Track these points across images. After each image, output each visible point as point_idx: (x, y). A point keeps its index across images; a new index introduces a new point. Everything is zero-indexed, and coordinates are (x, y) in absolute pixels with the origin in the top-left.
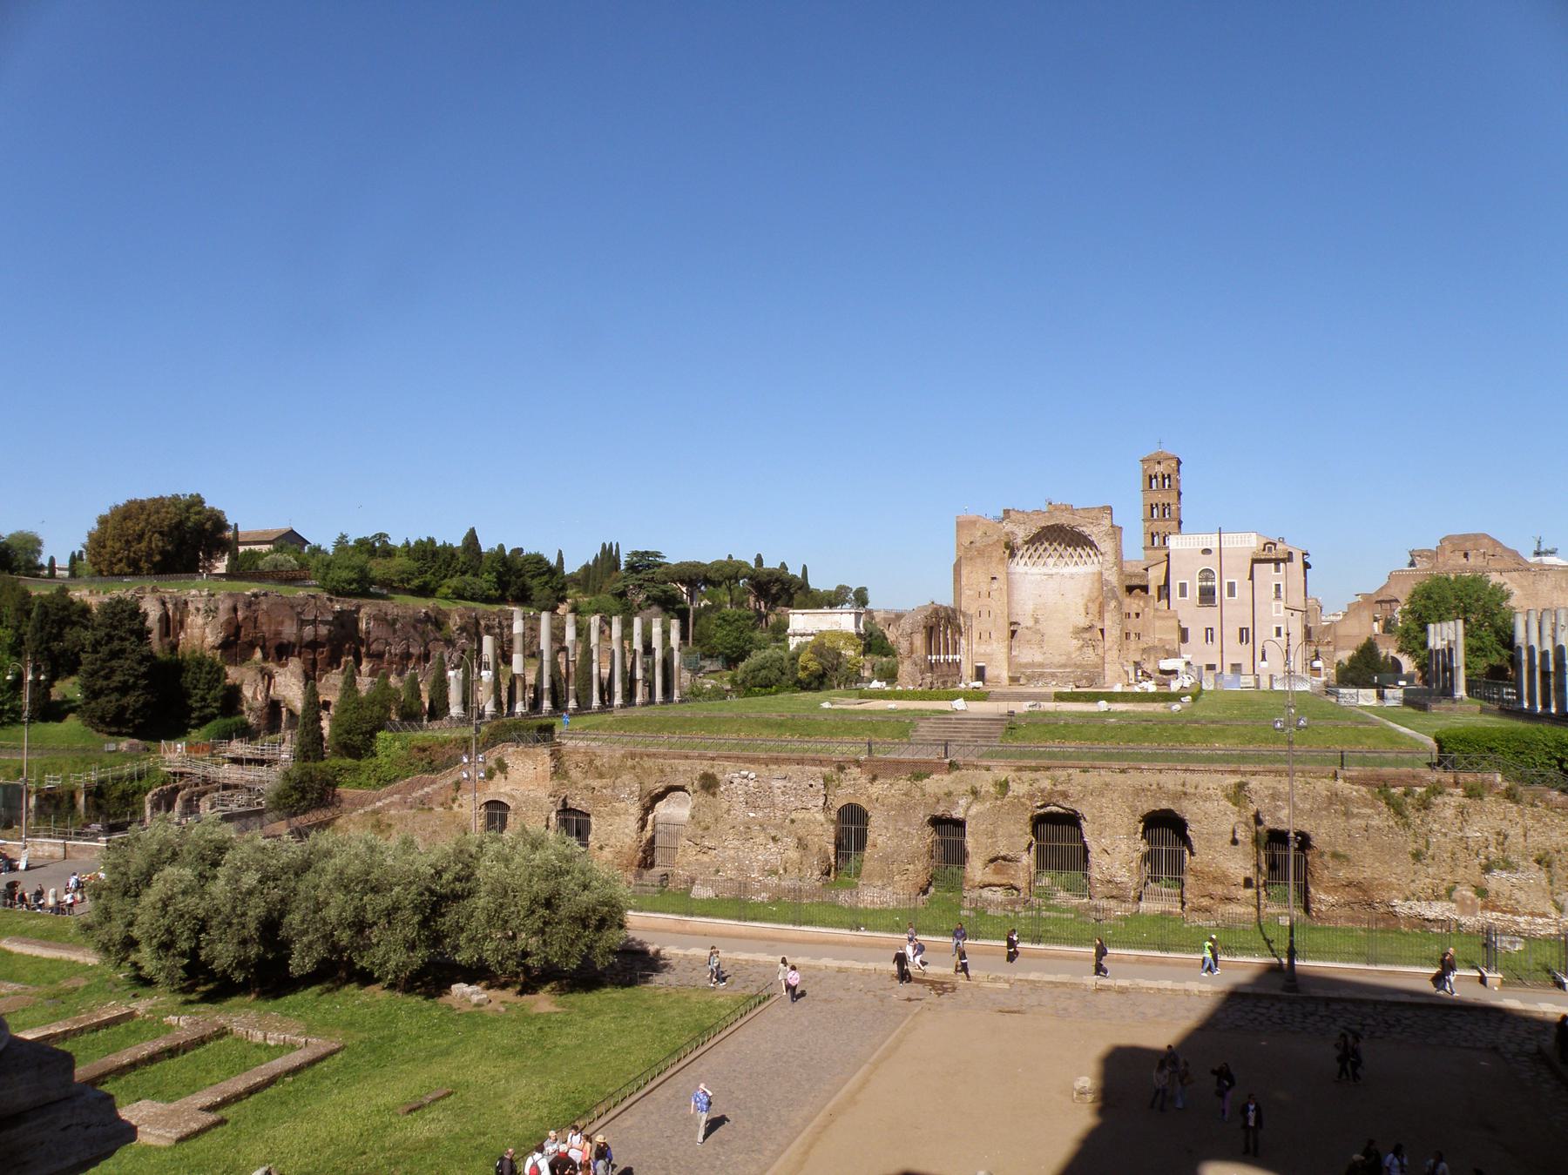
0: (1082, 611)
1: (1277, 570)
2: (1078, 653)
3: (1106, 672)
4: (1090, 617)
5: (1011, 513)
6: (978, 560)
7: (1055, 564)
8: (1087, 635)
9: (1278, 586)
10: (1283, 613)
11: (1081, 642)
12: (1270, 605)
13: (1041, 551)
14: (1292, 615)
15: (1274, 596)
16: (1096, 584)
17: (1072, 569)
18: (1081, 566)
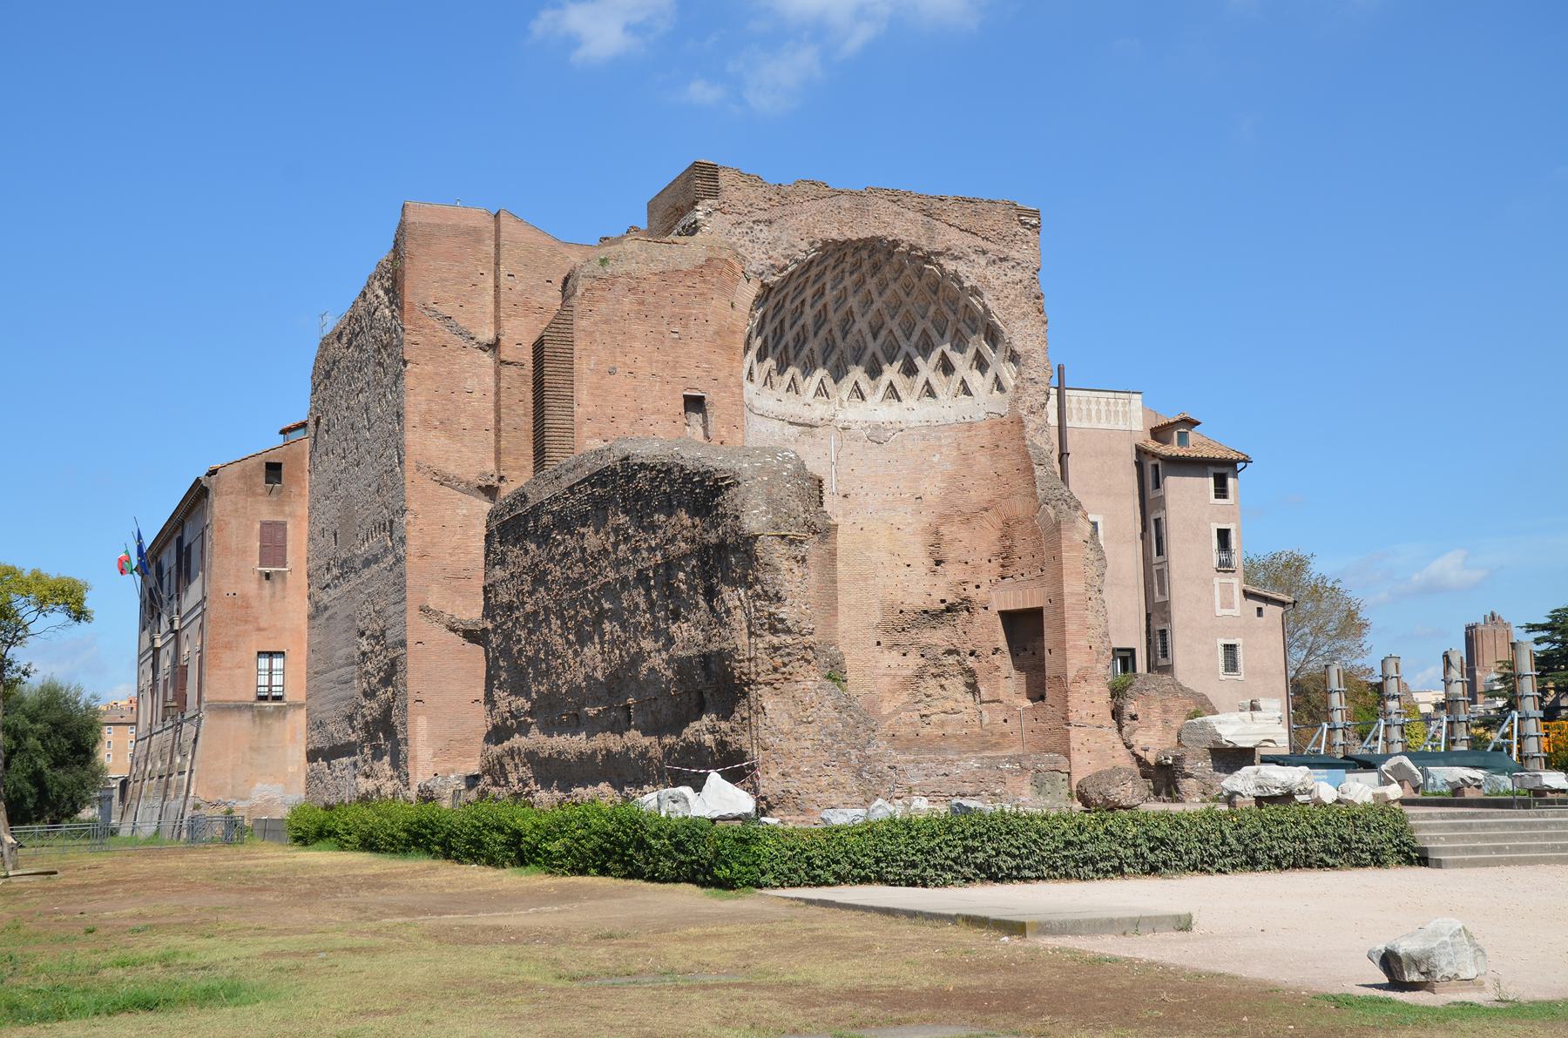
0: (922, 561)
1: (1221, 491)
2: (904, 697)
3: (1075, 756)
4: (952, 572)
5: (724, 180)
6: (638, 328)
7: (821, 391)
8: (939, 637)
9: (1223, 535)
10: (1242, 608)
11: (913, 661)
12: (1208, 583)
13: (789, 336)
14: (1260, 610)
15: (1215, 557)
16: (983, 461)
17: (875, 410)
18: (909, 401)
